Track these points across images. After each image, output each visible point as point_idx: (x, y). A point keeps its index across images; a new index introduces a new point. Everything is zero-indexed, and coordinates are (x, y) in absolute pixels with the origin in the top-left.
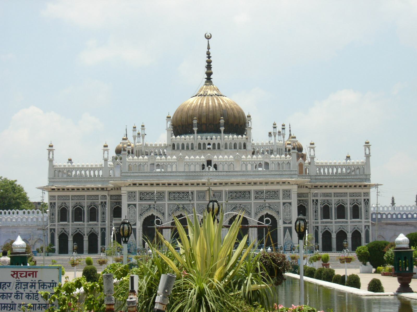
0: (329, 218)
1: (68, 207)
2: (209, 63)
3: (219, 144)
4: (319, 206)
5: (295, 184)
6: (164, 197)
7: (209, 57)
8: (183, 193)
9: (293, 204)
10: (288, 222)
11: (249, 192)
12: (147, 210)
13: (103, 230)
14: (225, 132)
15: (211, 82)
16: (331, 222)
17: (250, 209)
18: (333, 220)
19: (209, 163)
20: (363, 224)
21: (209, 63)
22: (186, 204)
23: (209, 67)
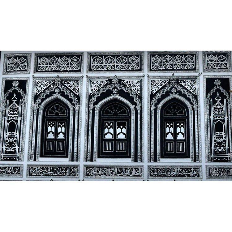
1: (74, 100)
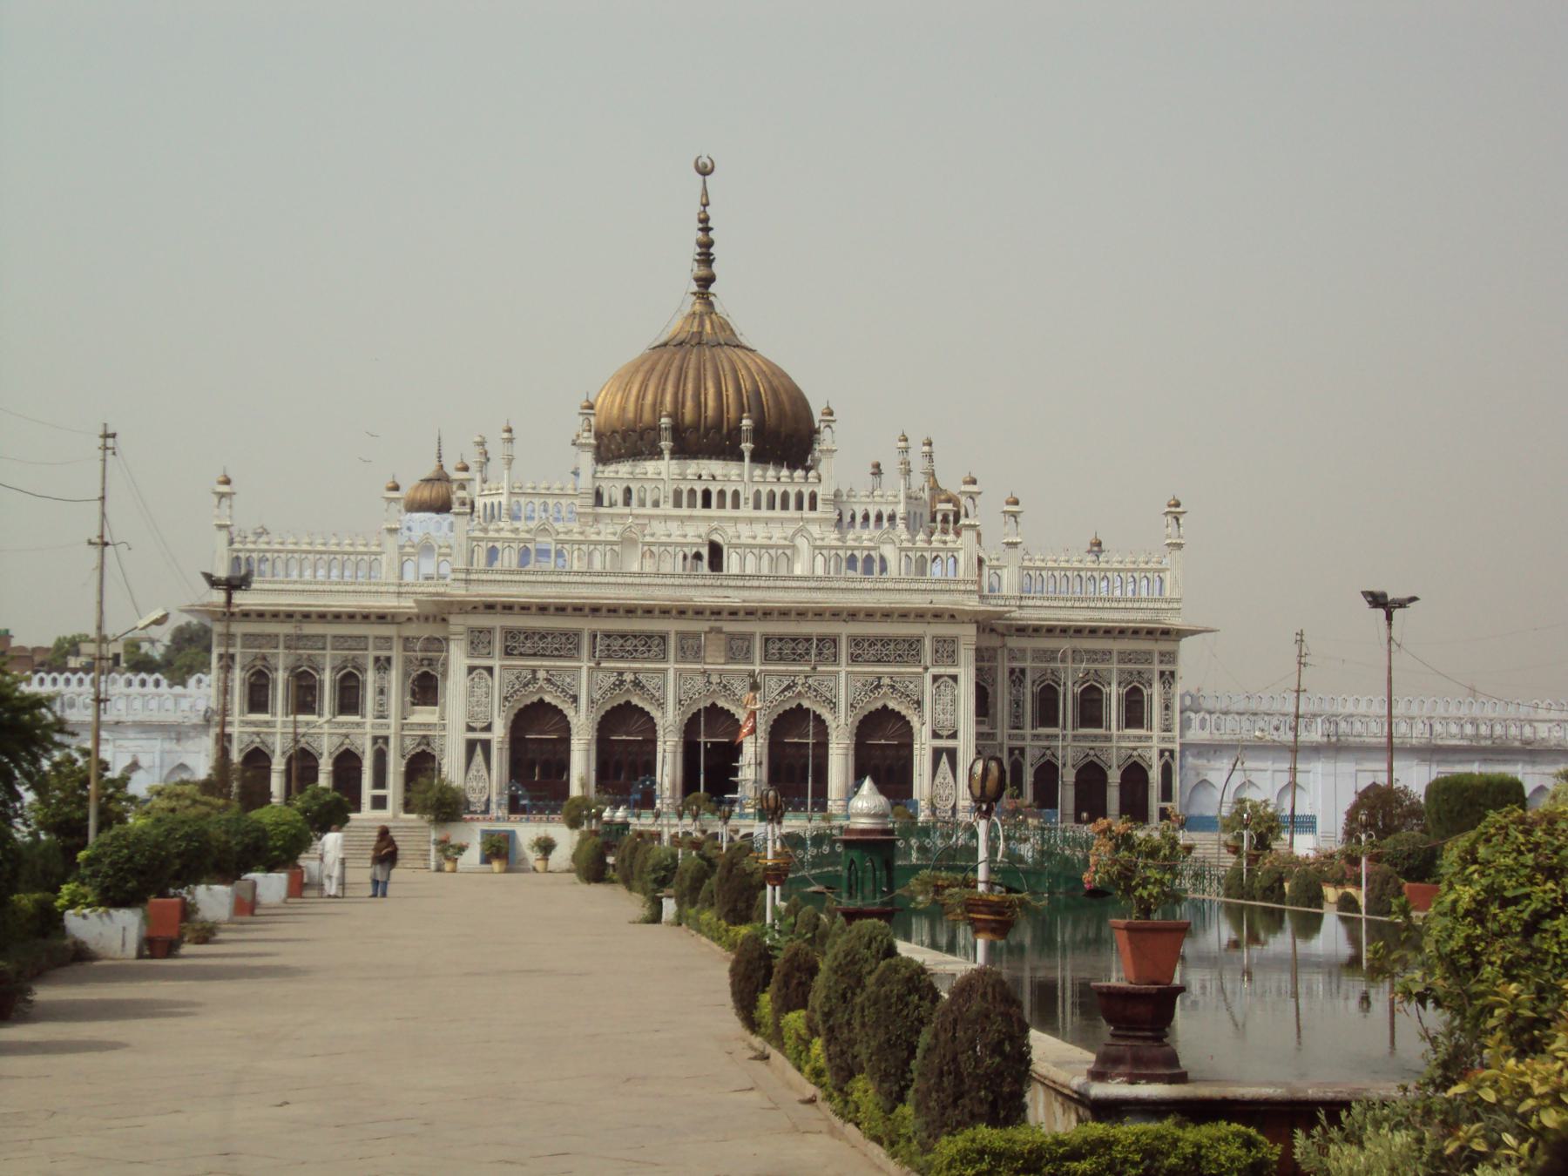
2: (706, 247)
3: (736, 494)
4: (1028, 691)
5: (970, 622)
6: (578, 648)
7: (706, 230)
9: (962, 680)
10: (945, 733)
11: (834, 641)
12: (526, 685)
13: (381, 742)
14: (759, 457)
15: (711, 304)
19: (716, 551)
20: (1156, 745)
21: (706, 247)
23: (706, 258)
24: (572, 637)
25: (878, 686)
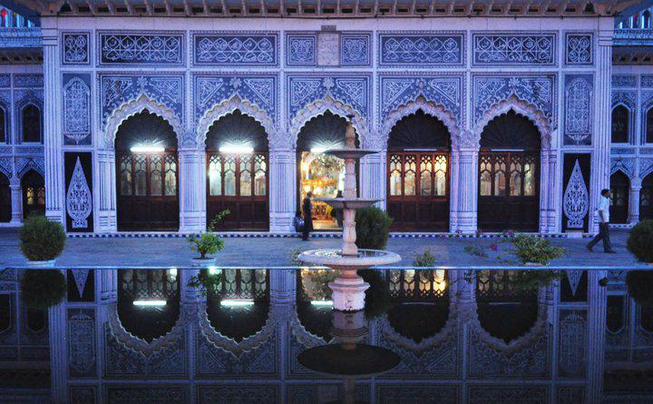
0: (625, 140)
6: (180, 51)
8: (243, 39)
16: (632, 151)
17: (458, 95)
18: (638, 146)
22: (251, 75)
24: (173, 39)
25: (506, 88)
